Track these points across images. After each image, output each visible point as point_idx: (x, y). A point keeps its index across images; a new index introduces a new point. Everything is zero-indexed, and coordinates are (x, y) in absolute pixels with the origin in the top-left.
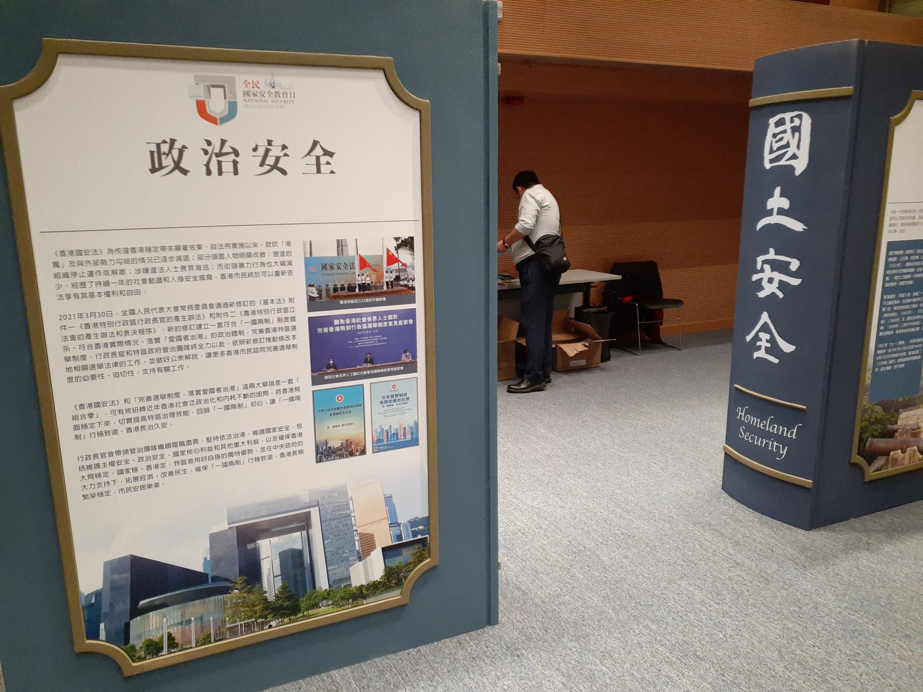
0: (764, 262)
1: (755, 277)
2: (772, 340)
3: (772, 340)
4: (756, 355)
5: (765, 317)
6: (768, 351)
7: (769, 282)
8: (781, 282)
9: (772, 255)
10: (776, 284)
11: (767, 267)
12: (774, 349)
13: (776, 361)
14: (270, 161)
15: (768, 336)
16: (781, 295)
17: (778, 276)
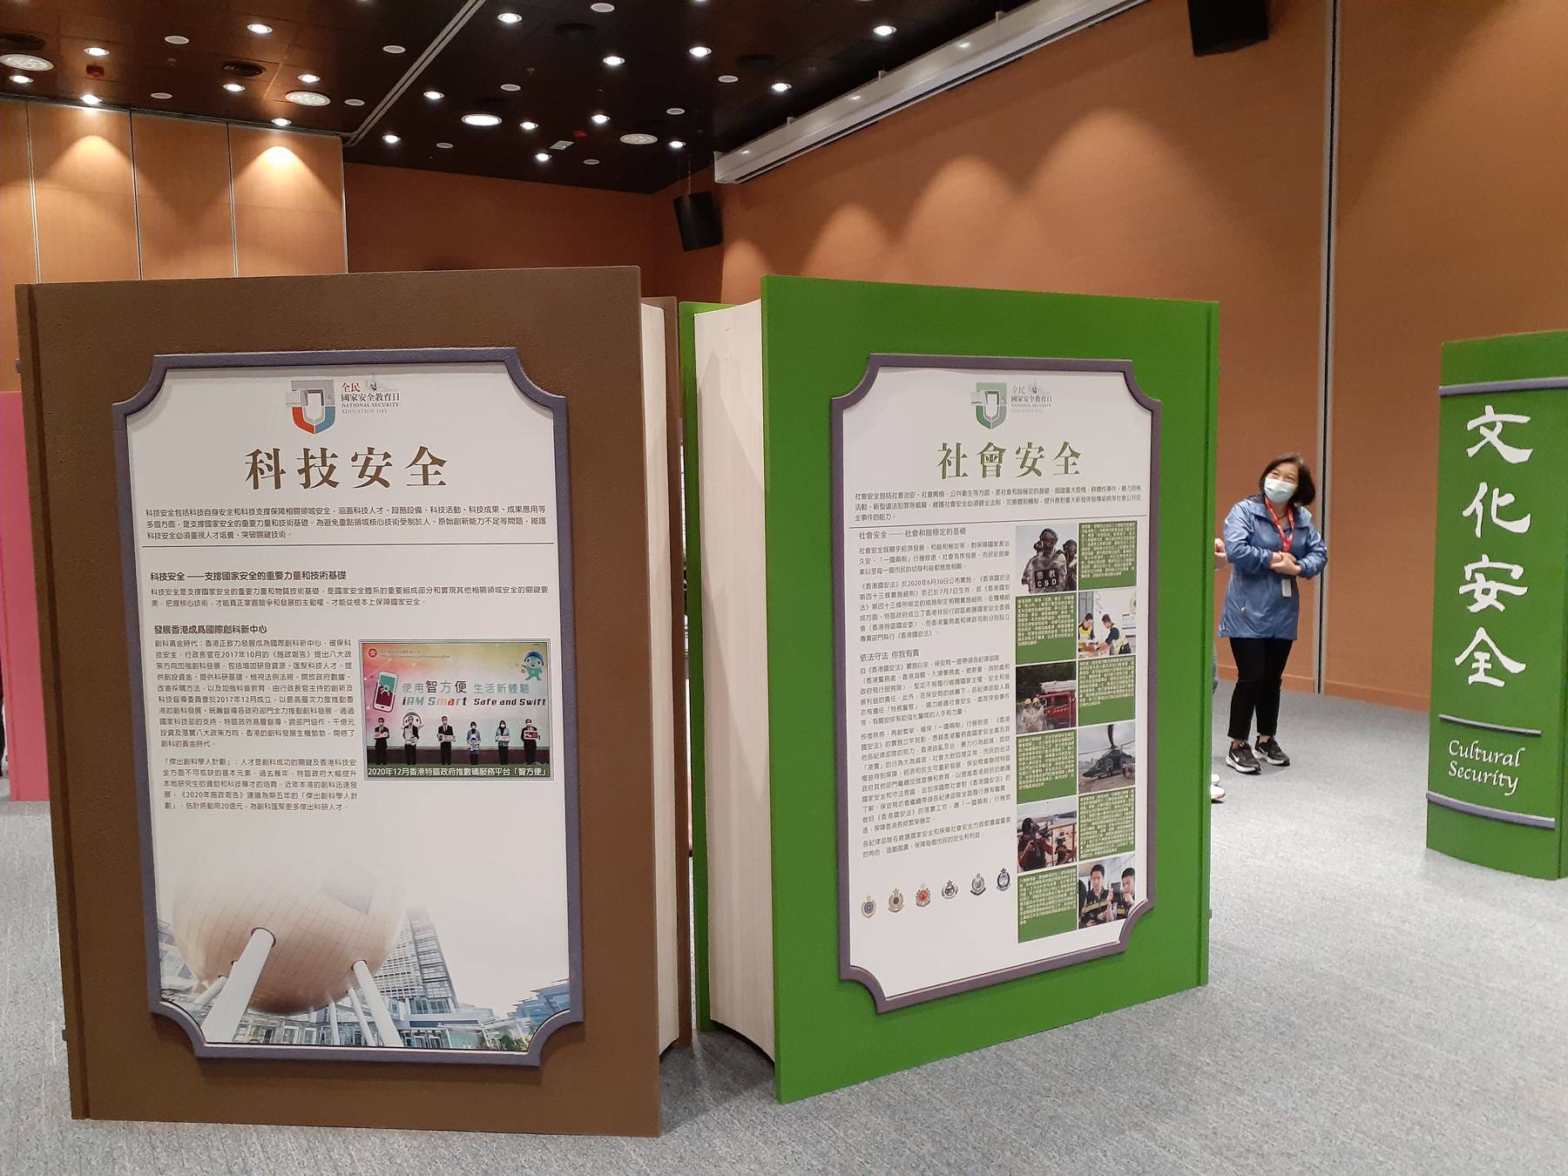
0: (1474, 572)
1: (1463, 590)
2: (1493, 659)
3: (1493, 659)
4: (1471, 679)
5: (1481, 634)
7: (1484, 594)
9: (1485, 562)
10: (1493, 594)
11: (1480, 577)
12: (1496, 670)
13: (1501, 684)
14: (1029, 463)
16: (1501, 608)
17: (1495, 587)
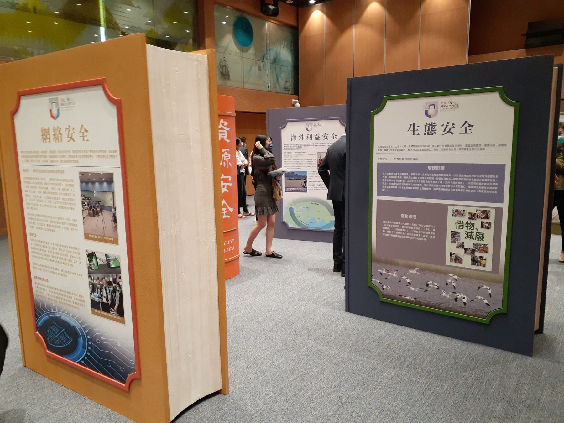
2: (227, 210)
3: (227, 210)
6: (226, 214)
8: (227, 186)
10: (226, 187)
12: (228, 213)
15: (225, 209)
16: (228, 191)
17: (226, 184)
